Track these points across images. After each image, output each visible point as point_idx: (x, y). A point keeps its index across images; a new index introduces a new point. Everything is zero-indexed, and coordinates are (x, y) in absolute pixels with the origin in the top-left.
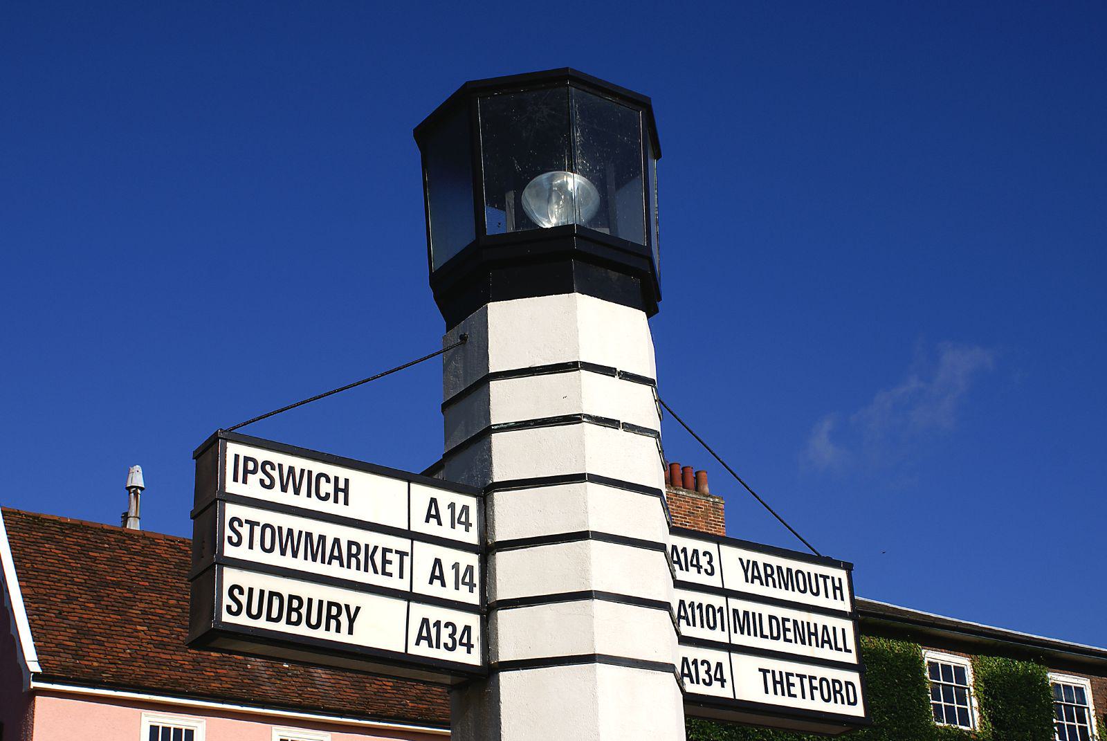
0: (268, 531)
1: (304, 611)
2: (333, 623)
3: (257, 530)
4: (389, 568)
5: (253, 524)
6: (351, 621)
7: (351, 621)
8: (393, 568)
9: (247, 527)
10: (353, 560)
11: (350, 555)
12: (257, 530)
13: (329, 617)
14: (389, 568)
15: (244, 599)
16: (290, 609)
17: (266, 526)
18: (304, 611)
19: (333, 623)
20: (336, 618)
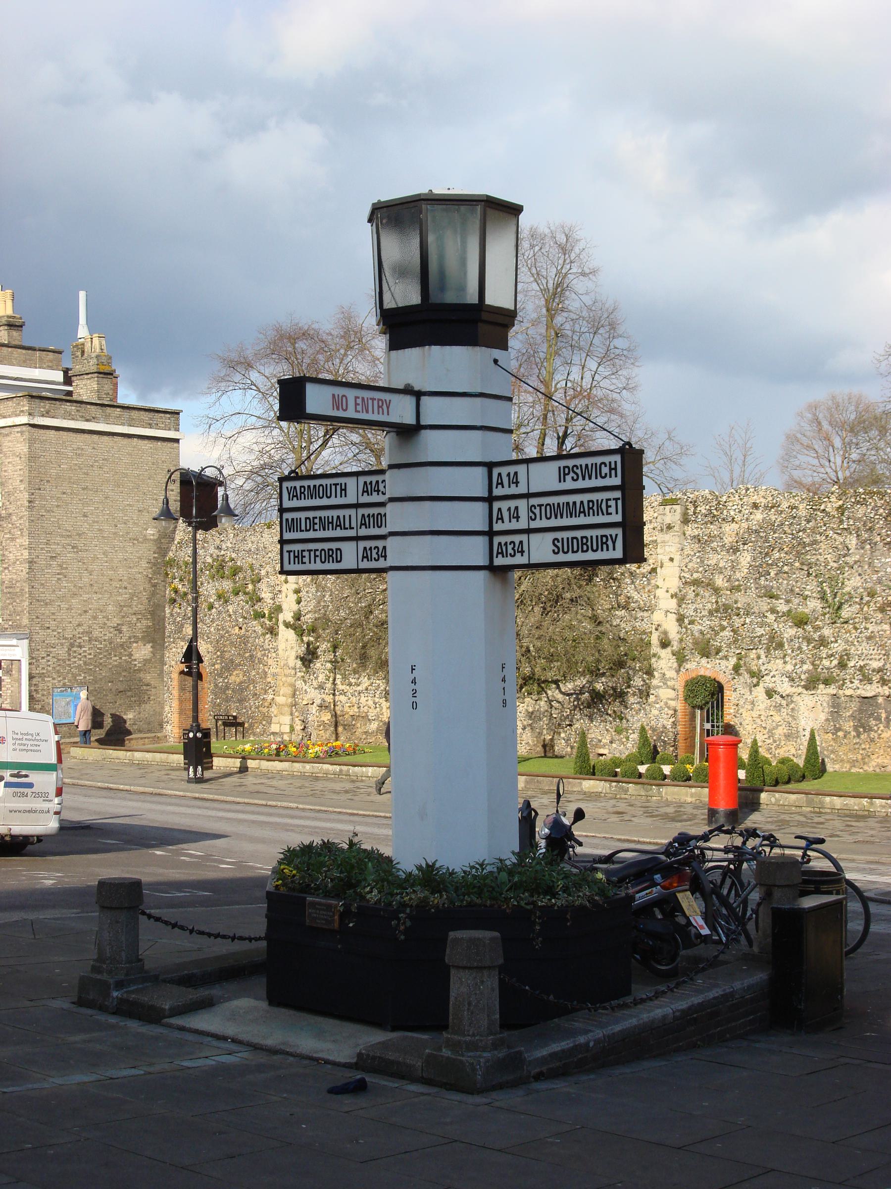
0: (548, 507)
1: (589, 543)
2: (605, 546)
3: (543, 508)
4: (610, 510)
5: (540, 506)
6: (614, 543)
7: (614, 543)
8: (612, 510)
9: (538, 508)
10: (591, 511)
11: (589, 508)
12: (543, 508)
13: (602, 543)
14: (610, 510)
15: (560, 545)
16: (583, 544)
17: (547, 505)
18: (589, 543)
19: (605, 546)
20: (606, 543)
